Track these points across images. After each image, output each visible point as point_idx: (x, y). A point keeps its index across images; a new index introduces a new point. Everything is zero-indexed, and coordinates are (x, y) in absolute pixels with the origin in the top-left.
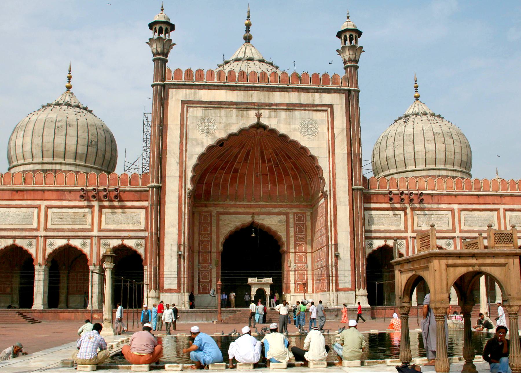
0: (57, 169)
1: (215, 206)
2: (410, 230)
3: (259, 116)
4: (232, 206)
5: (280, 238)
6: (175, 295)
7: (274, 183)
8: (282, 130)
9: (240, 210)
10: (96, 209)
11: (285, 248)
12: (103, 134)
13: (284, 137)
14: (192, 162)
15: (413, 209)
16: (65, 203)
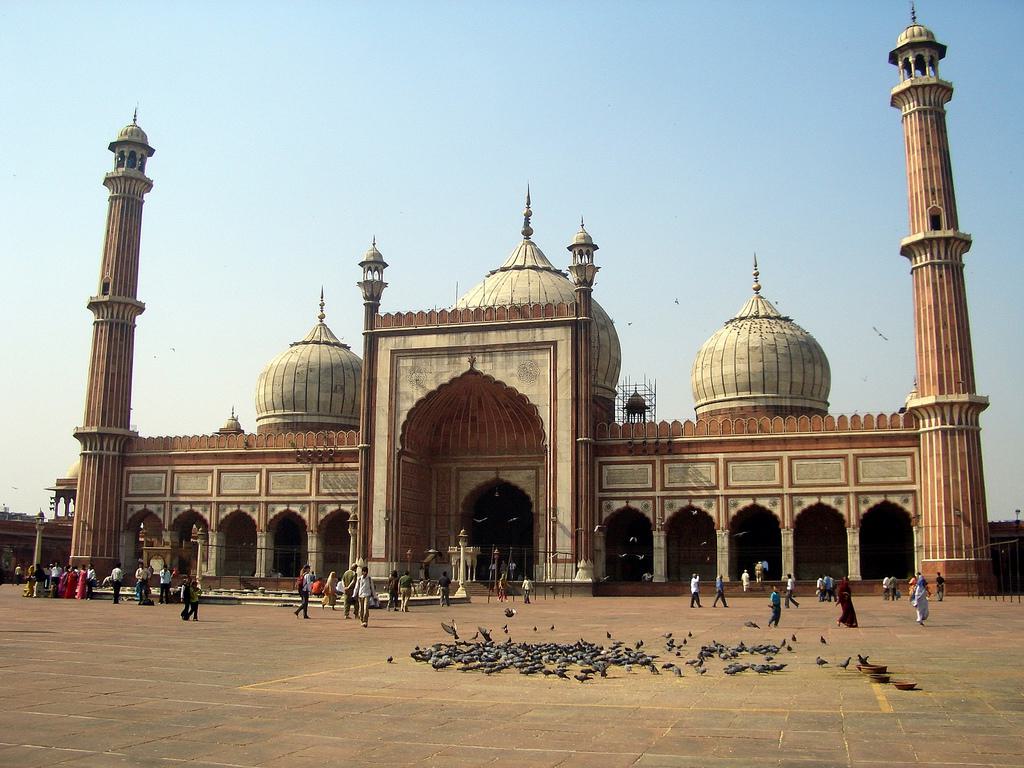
0: (299, 421)
1: (456, 461)
2: (658, 488)
3: (472, 362)
4: (476, 460)
5: (528, 497)
6: (383, 566)
7: (520, 431)
8: (499, 375)
9: (482, 465)
10: (314, 472)
11: (534, 510)
12: (352, 376)
13: (500, 384)
14: (403, 418)
15: (663, 462)
16: (284, 466)
